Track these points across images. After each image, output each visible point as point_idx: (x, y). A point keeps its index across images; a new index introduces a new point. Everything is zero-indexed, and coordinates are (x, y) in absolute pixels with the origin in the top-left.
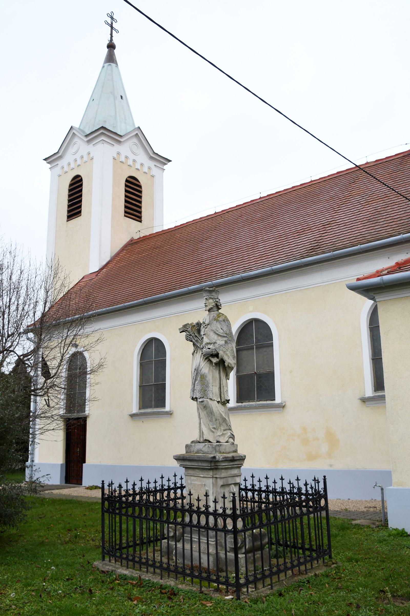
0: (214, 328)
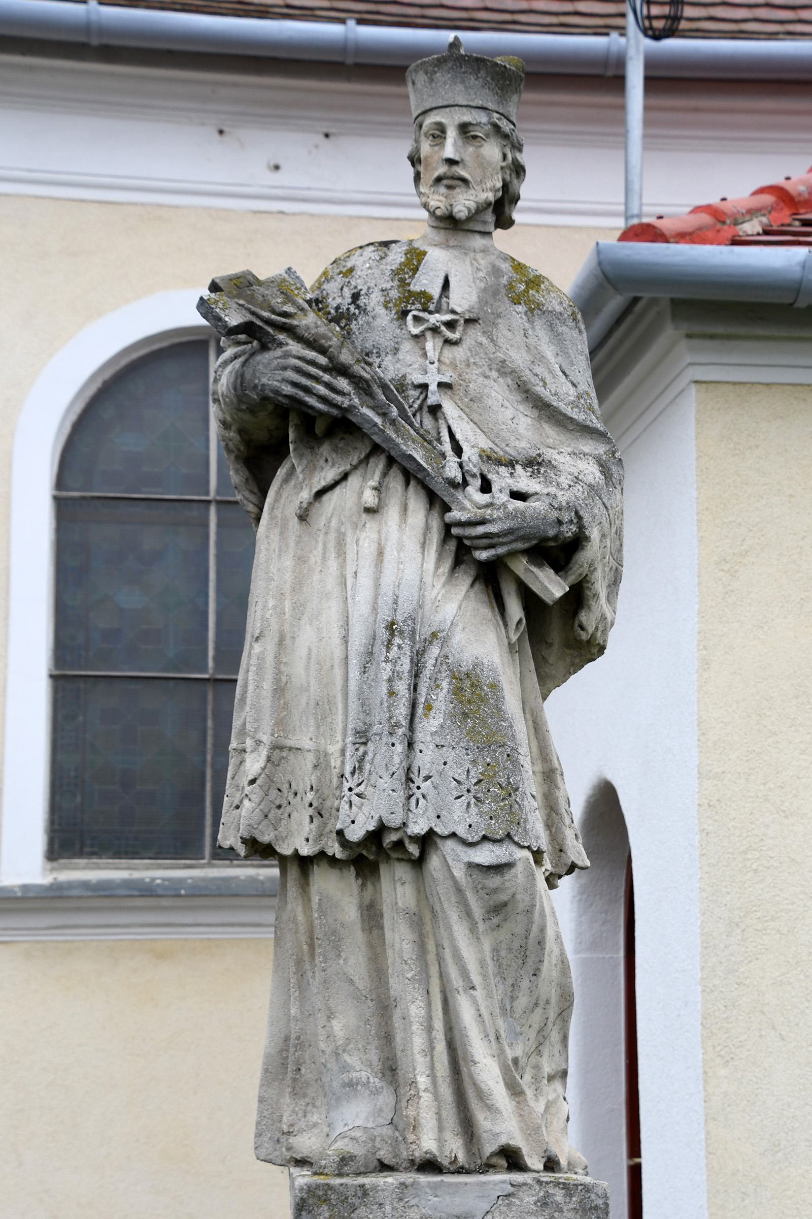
0: (519, 358)
